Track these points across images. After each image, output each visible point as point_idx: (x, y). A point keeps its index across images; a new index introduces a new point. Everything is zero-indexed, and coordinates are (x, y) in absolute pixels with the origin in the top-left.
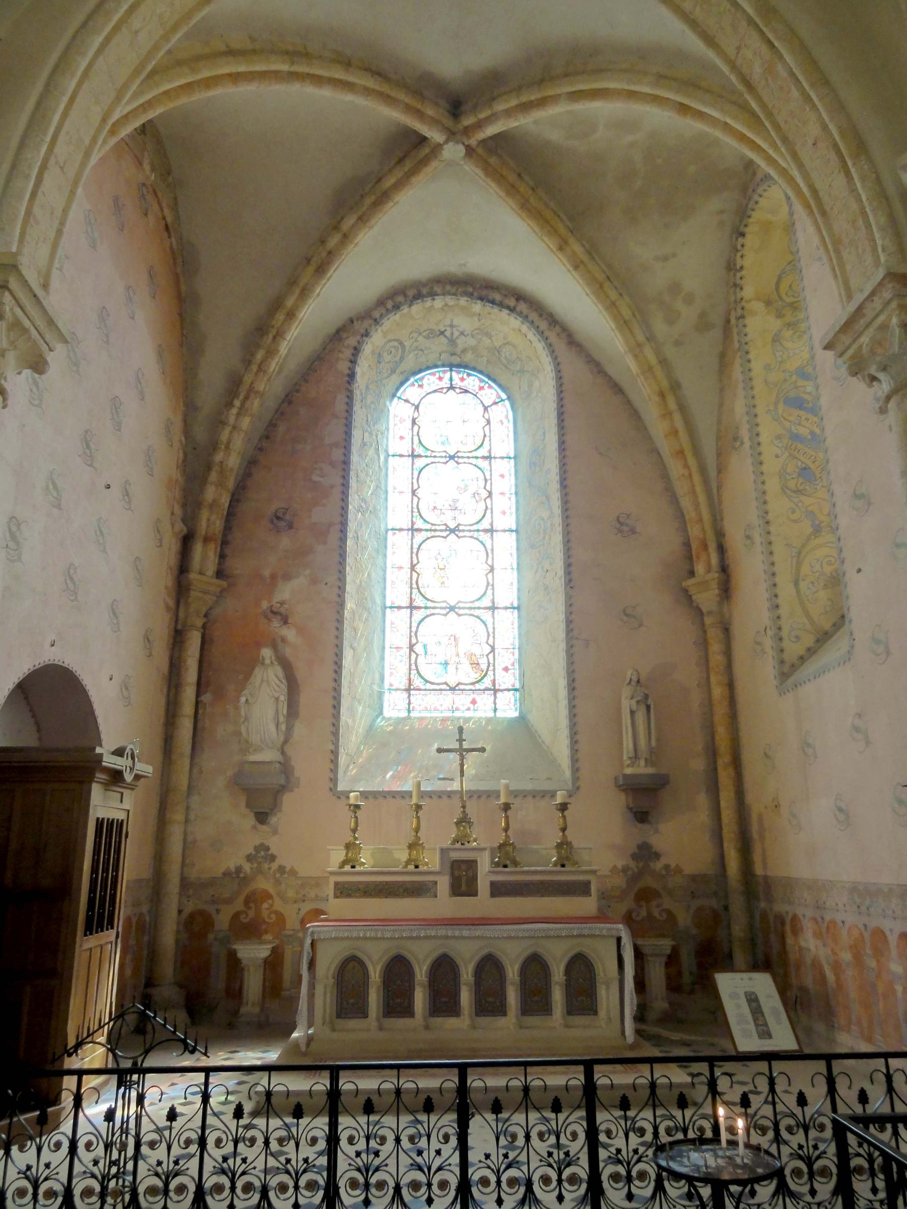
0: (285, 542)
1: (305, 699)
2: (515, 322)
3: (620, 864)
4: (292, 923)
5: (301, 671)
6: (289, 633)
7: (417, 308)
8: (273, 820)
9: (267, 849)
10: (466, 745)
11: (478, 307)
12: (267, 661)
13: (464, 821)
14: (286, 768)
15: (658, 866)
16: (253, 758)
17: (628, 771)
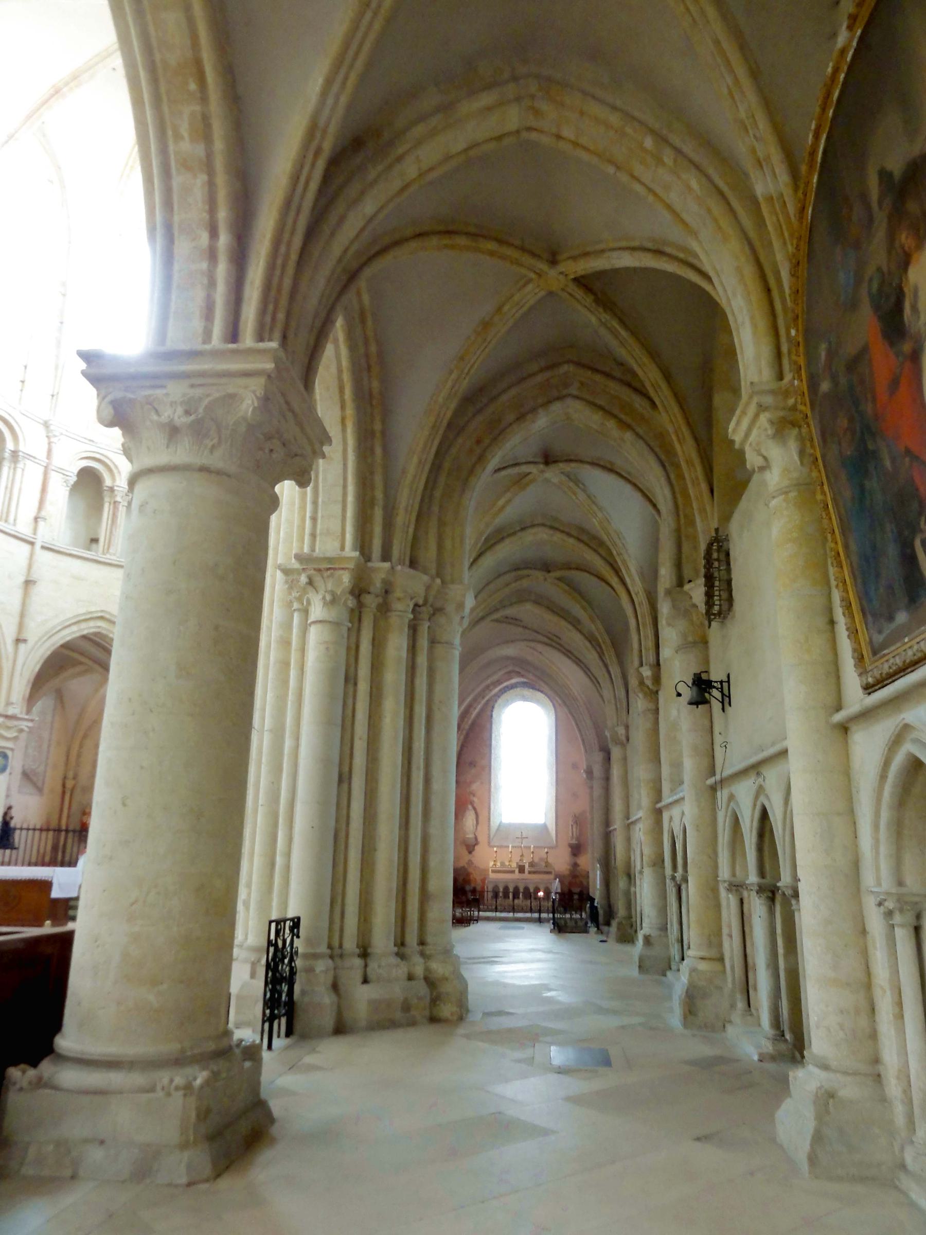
0: (473, 771)
1: (480, 818)
2: (542, 695)
3: (569, 867)
4: (479, 881)
5: (478, 810)
6: (475, 799)
7: (511, 691)
8: (473, 853)
9: (471, 861)
10: (523, 836)
11: (531, 690)
12: (470, 809)
13: (522, 856)
14: (476, 838)
15: (578, 868)
16: (467, 836)
17: (571, 842)
